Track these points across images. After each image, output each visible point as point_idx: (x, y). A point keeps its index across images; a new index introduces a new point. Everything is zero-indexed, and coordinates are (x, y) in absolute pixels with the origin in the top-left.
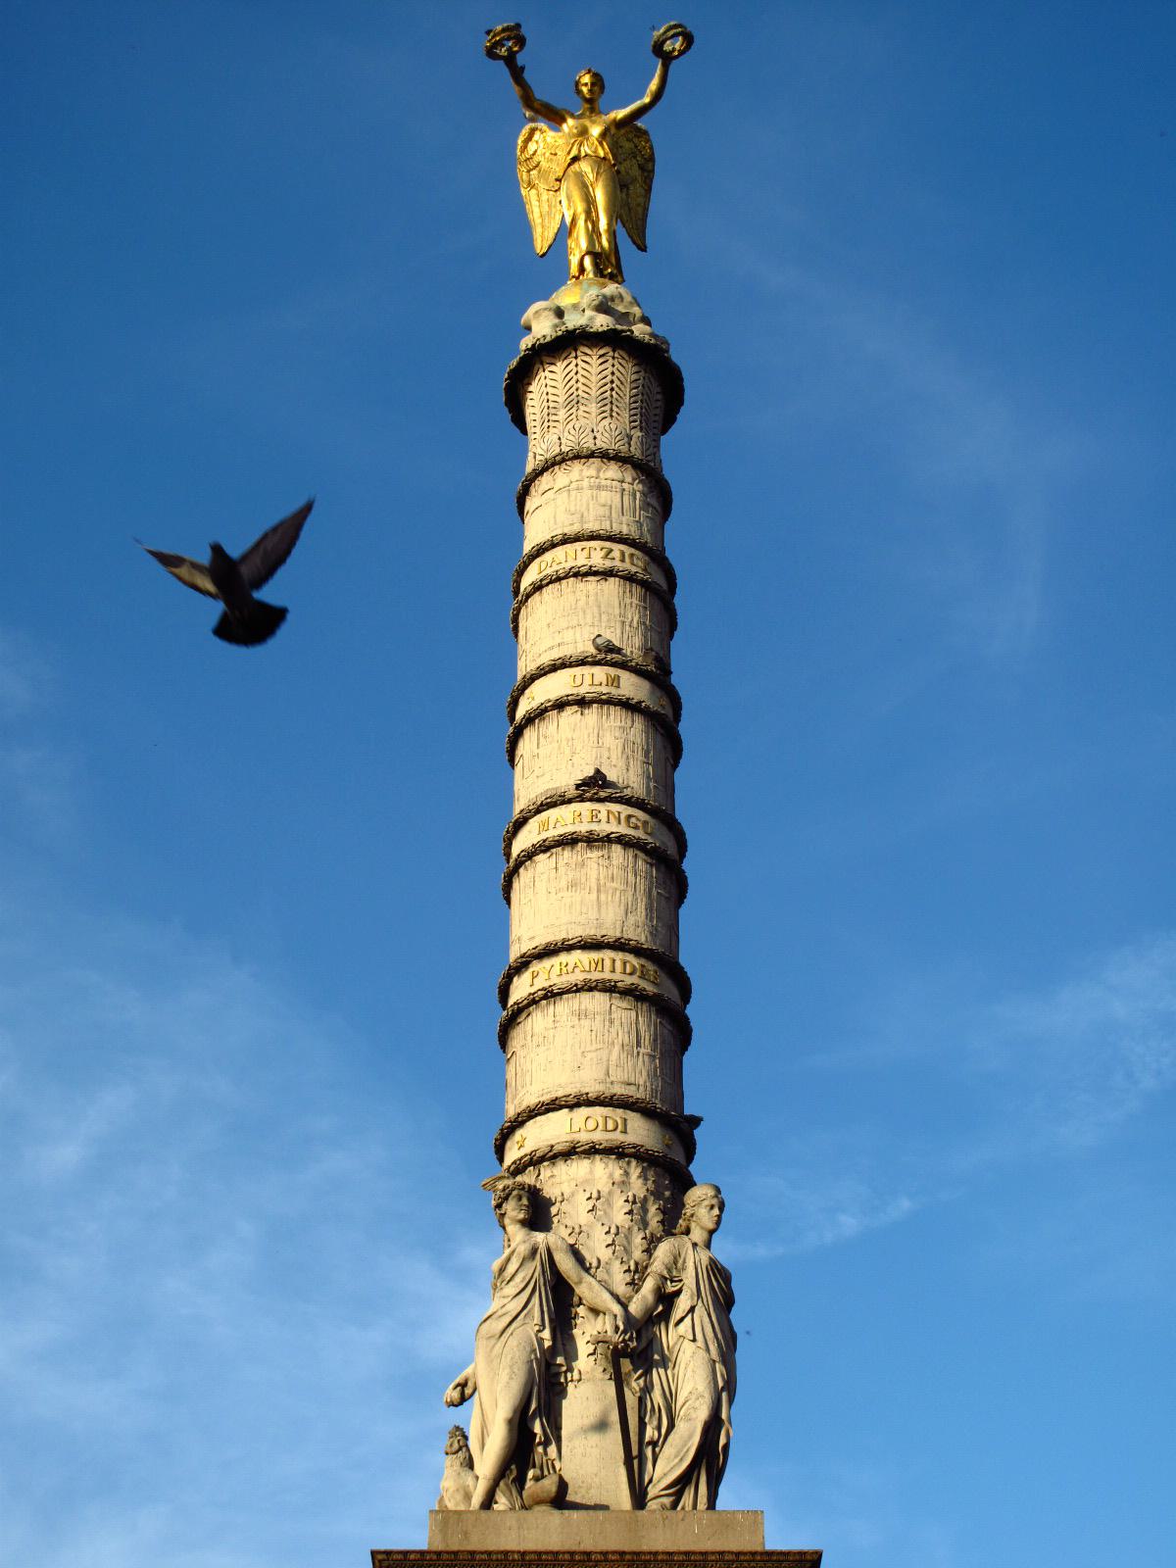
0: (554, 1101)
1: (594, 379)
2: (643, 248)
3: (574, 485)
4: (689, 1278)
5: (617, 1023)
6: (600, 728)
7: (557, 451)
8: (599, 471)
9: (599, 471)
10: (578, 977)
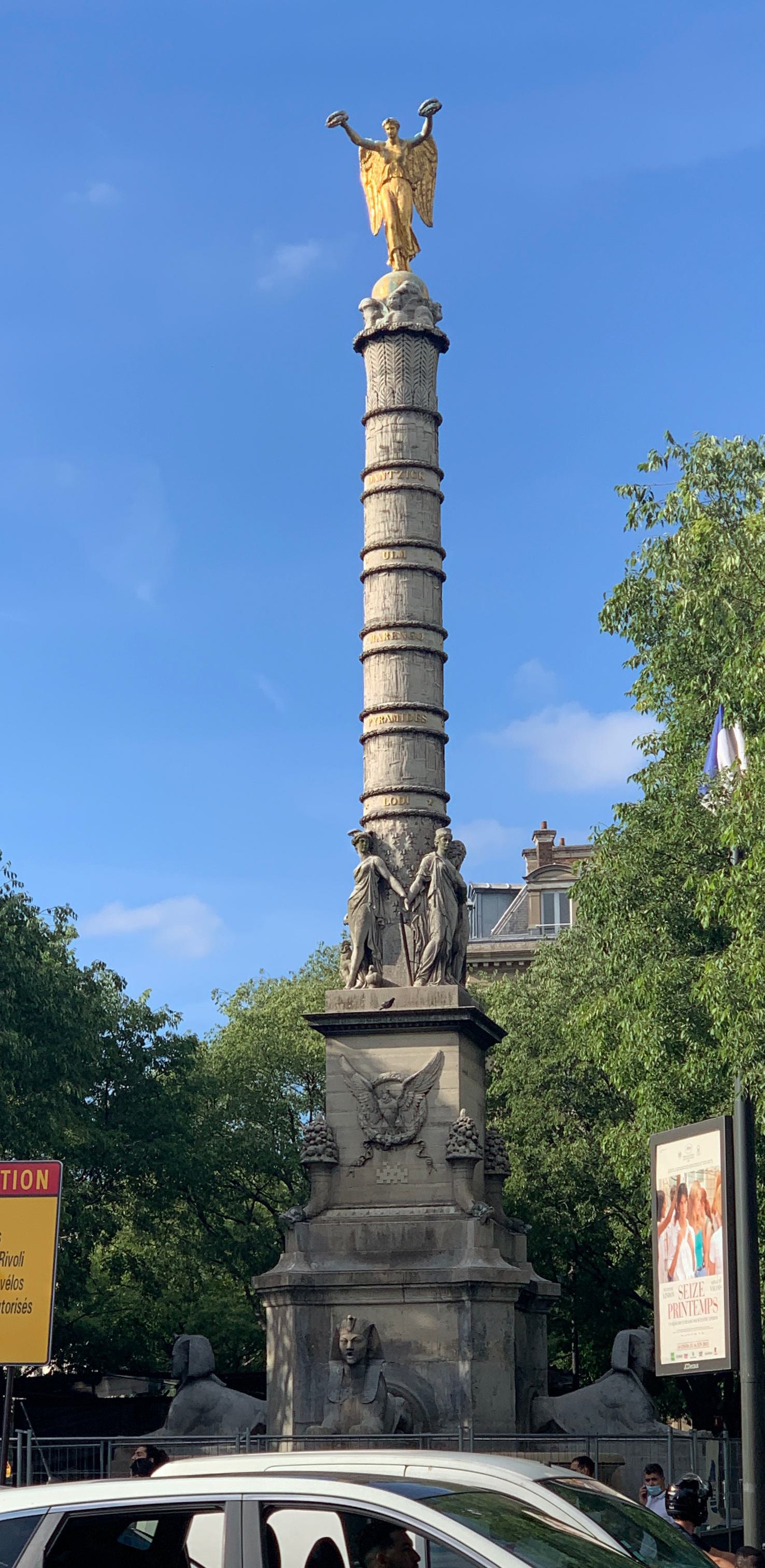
1: (393, 356)
3: (384, 429)
4: (433, 876)
5: (405, 748)
6: (397, 583)
10: (387, 727)
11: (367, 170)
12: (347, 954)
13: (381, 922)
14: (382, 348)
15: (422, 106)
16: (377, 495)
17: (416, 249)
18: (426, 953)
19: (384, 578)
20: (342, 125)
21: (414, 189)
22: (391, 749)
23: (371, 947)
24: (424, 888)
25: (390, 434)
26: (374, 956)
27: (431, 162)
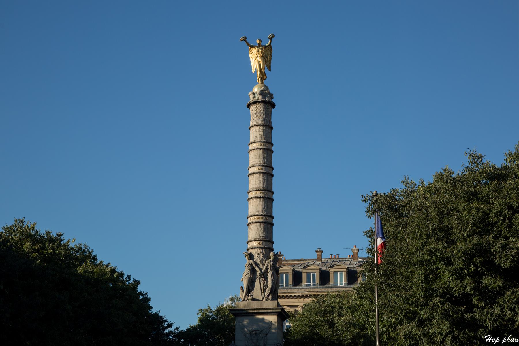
2: (270, 70)
3: (256, 131)
4: (269, 267)
5: (261, 227)
6: (259, 177)
10: (256, 221)
11: (251, 54)
12: (242, 290)
15: (269, 36)
16: (253, 150)
17: (266, 77)
20: (245, 40)
21: (266, 60)
22: (257, 227)
23: (250, 288)
25: (258, 132)
27: (270, 52)
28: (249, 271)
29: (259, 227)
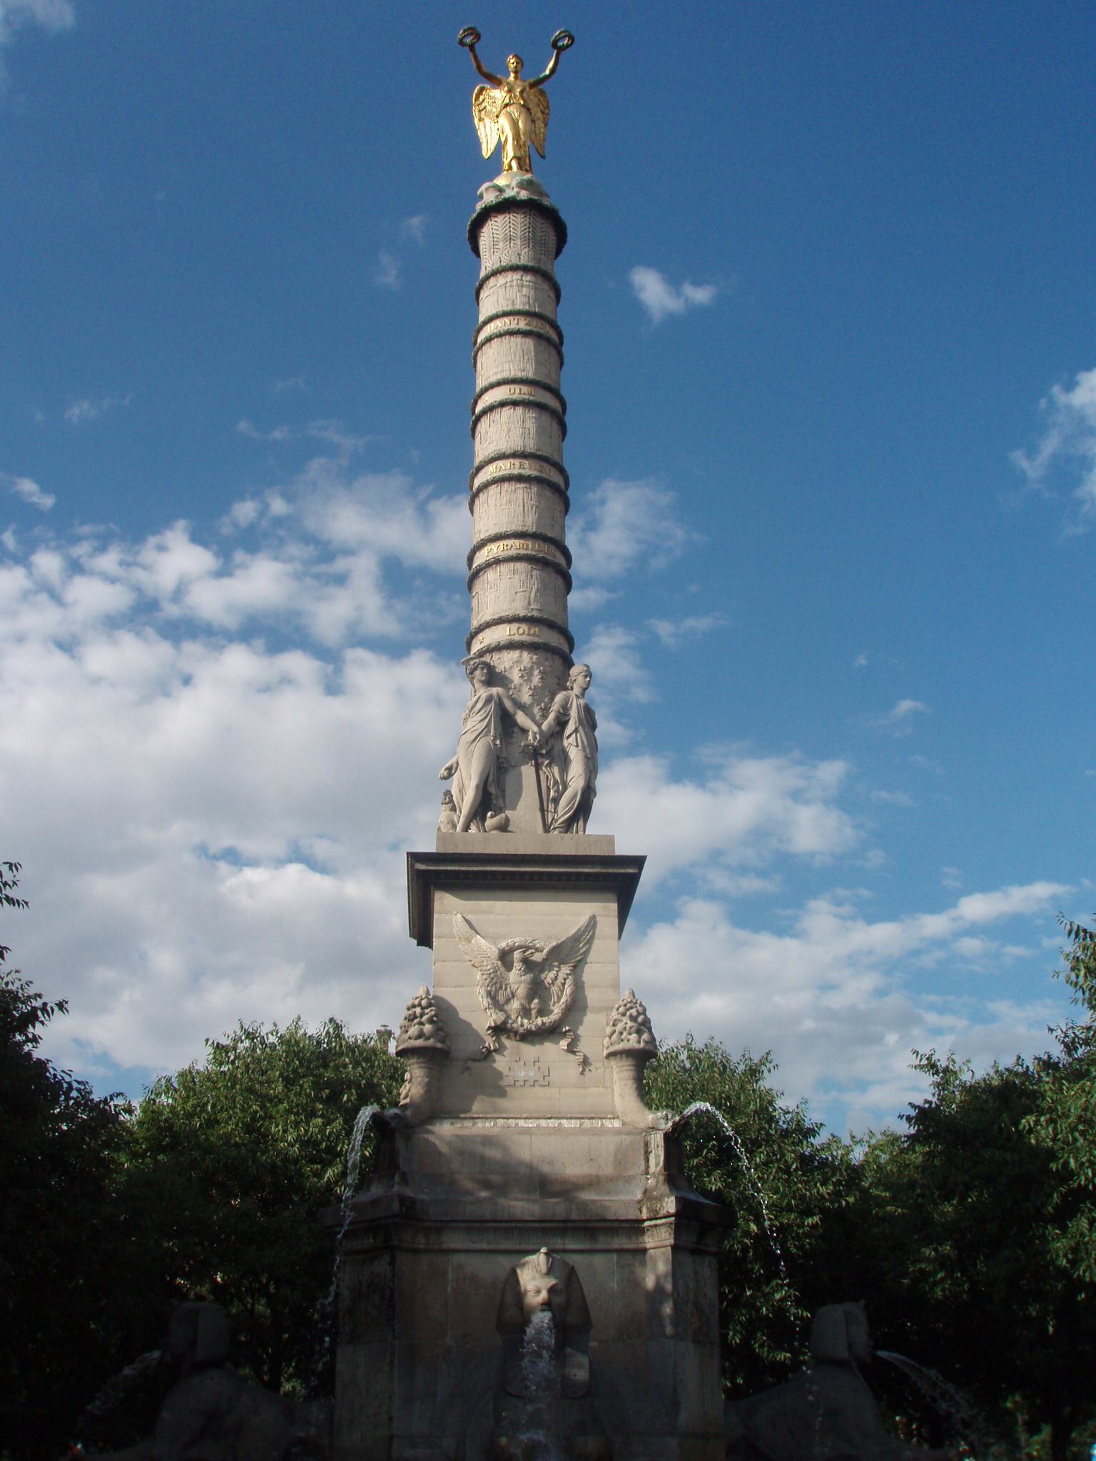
0: (500, 618)
3: (508, 284)
4: (573, 713)
5: (534, 577)
7: (499, 265)
8: (522, 277)
9: (522, 277)
10: (513, 552)
11: (480, 111)
12: (450, 805)
13: (503, 763)
14: (507, 218)
16: (499, 339)
18: (563, 802)
19: (508, 412)
22: (517, 577)
23: (492, 790)
24: (558, 729)
25: (516, 289)
26: (495, 802)
28: (491, 717)
29: (524, 574)
